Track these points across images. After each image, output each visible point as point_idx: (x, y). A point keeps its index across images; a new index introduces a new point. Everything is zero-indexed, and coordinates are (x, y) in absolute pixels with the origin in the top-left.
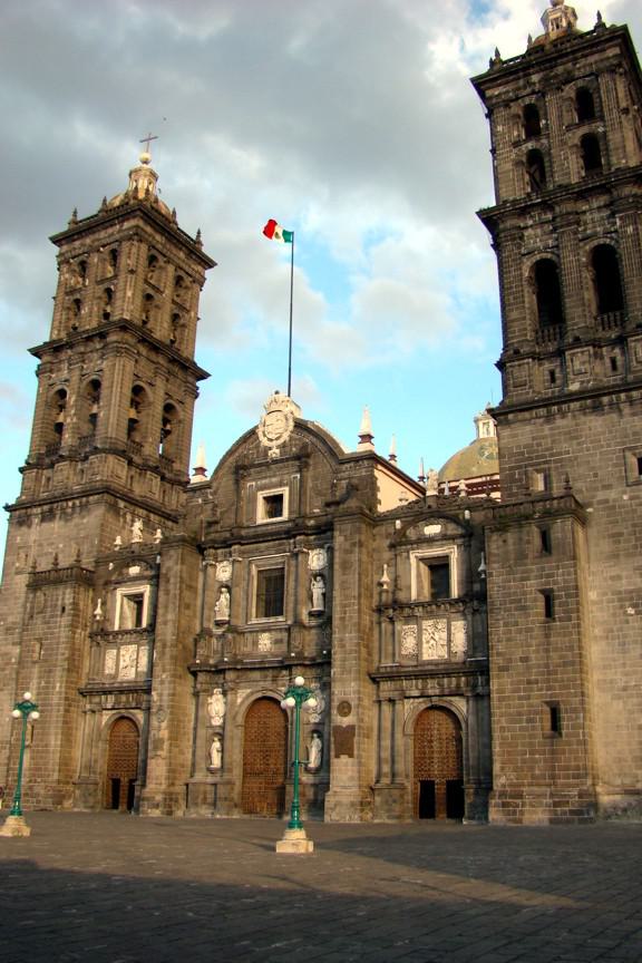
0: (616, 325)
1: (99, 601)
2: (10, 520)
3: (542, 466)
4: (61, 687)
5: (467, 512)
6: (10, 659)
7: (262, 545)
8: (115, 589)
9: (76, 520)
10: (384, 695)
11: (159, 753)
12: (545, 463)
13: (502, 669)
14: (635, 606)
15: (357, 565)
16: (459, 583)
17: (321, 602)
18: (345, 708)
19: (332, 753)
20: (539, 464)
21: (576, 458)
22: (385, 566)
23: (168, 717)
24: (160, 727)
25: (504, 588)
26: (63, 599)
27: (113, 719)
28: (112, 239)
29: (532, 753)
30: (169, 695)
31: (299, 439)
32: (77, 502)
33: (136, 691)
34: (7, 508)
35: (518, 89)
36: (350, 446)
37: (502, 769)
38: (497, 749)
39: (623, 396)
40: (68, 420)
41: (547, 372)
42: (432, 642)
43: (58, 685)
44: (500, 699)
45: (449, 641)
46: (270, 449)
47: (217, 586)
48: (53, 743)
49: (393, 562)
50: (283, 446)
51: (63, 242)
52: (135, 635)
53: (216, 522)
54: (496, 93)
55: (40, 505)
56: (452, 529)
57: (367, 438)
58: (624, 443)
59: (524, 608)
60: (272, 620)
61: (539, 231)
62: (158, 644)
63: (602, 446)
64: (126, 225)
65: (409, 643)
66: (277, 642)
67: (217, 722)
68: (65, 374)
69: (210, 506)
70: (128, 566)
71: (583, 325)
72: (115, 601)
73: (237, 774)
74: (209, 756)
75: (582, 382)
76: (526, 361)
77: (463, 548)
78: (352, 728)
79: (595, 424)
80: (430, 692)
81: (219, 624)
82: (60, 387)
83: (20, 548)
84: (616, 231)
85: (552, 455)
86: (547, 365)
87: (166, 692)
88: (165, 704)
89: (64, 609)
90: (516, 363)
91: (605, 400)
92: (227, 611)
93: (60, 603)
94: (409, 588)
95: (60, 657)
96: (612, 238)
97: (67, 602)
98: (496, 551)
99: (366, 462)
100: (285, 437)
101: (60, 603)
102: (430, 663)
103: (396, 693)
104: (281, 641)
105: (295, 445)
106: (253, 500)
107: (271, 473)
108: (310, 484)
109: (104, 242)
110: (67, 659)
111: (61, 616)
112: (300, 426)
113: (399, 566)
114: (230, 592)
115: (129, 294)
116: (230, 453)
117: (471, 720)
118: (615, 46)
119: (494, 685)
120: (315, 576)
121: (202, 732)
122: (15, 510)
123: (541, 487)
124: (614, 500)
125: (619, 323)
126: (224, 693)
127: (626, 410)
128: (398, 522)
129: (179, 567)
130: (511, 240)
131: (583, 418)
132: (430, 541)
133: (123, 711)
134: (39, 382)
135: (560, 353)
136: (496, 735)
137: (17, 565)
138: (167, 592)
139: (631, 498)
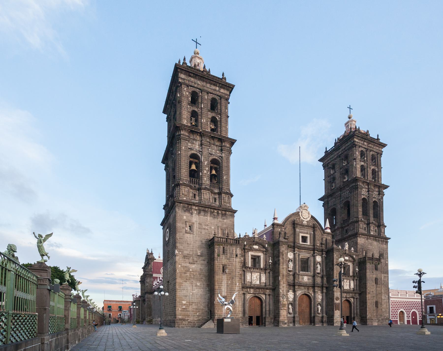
8: (248, 252)
13: (369, 293)
26: (236, 251)
40: (205, 172)
43: (238, 284)
48: (238, 304)
50: (307, 222)
59: (373, 281)
69: (283, 233)
89: (237, 256)
93: (234, 252)
95: (237, 273)
100: (309, 219)
101: (234, 252)
106: (299, 236)
110: (241, 275)
111: (236, 258)
112: (312, 217)
119: (367, 296)
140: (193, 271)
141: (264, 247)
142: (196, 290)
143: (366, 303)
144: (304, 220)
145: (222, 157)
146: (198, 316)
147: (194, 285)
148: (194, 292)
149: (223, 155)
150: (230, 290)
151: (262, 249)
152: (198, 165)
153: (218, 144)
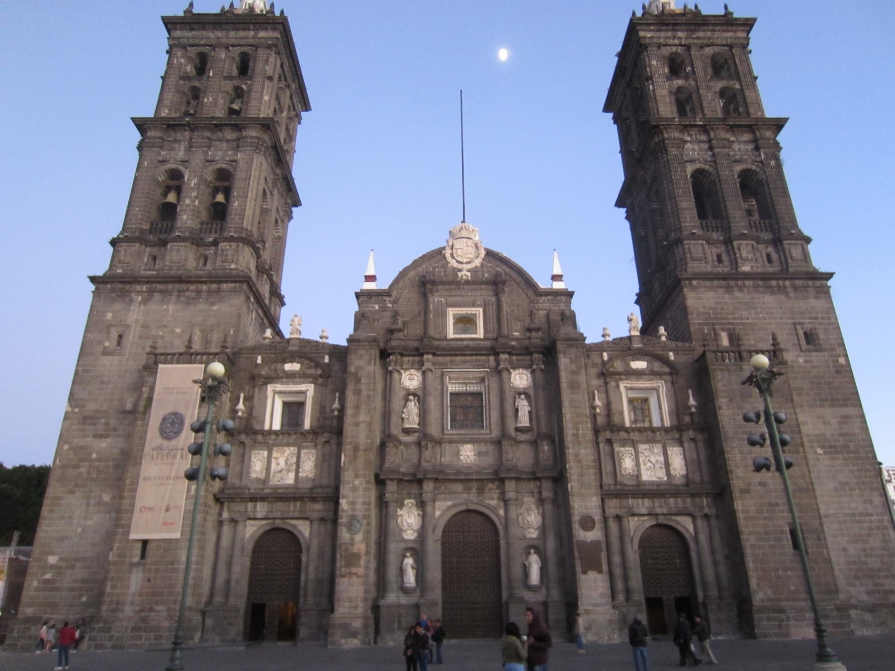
0: (766, 231)
1: (242, 395)
2: (96, 293)
3: (727, 326)
5: (671, 354)
6: (90, 454)
7: (459, 358)
8: (266, 384)
9: (201, 306)
10: (611, 511)
11: (354, 570)
12: (730, 323)
13: (746, 491)
14: (822, 447)
15: (585, 385)
16: (670, 414)
17: (527, 418)
18: (588, 523)
19: (578, 569)
20: (726, 324)
21: (756, 324)
22: (596, 392)
23: (364, 528)
24: (352, 540)
25: (734, 419)
27: (261, 531)
28: (244, 42)
29: (785, 569)
30: (365, 503)
31: (492, 267)
32: (205, 287)
33: (301, 499)
34: (93, 279)
35: (669, 38)
36: (543, 283)
37: (758, 584)
38: (750, 565)
39: (787, 283)
40: (188, 201)
41: (714, 255)
42: (649, 464)
44: (745, 519)
45: (667, 465)
46: (460, 270)
47: (402, 393)
49: (603, 389)
50: (473, 271)
51: (178, 26)
52: (293, 437)
53: (400, 330)
54: (649, 35)
55: (147, 282)
56: (657, 366)
57: (556, 278)
58: (794, 319)
60: (475, 431)
61: (696, 147)
62: (347, 447)
63: (776, 318)
64: (262, 34)
65: (628, 464)
66: (479, 454)
67: (410, 535)
68: (181, 154)
69: (387, 314)
70: (284, 361)
71: (743, 224)
72: (266, 398)
73: (436, 594)
74: (402, 571)
75: (752, 267)
76: (700, 242)
77: (669, 384)
78: (596, 544)
79: (769, 300)
80: (658, 511)
81: (407, 431)
82: (174, 166)
83: (109, 326)
84: (761, 162)
85: (735, 319)
86: (715, 250)
87: (360, 501)
88: (359, 513)
90: (692, 242)
91: (774, 283)
92: (416, 419)
94: (622, 413)
96: (757, 166)
98: (722, 388)
99: (564, 298)
100: (477, 262)
102: (652, 483)
103: (623, 510)
104: (486, 453)
105: (487, 272)
106: (444, 315)
107: (463, 293)
108: (505, 308)
109: (232, 41)
112: (490, 254)
113: (612, 395)
114: (419, 401)
115: (266, 98)
116: (416, 264)
118: (743, 31)
119: (738, 505)
120: (520, 394)
121: (394, 548)
122: (105, 283)
123: (725, 342)
124: (792, 361)
125: (768, 229)
126: (421, 504)
127: (792, 294)
128: (605, 354)
129: (372, 367)
130: (677, 147)
131: (756, 296)
132: (638, 374)
133: (278, 522)
134: (140, 156)
135: (728, 242)
136: (748, 551)
137: (107, 344)
138: (358, 392)
139: (806, 361)
140: (98, 460)
141: (318, 365)
142: (96, 517)
144: (460, 266)
145: (236, 161)
146: (87, 605)
147: (92, 502)
148: (90, 523)
149: (240, 156)
151: (312, 371)
152: (179, 190)
153: (230, 135)
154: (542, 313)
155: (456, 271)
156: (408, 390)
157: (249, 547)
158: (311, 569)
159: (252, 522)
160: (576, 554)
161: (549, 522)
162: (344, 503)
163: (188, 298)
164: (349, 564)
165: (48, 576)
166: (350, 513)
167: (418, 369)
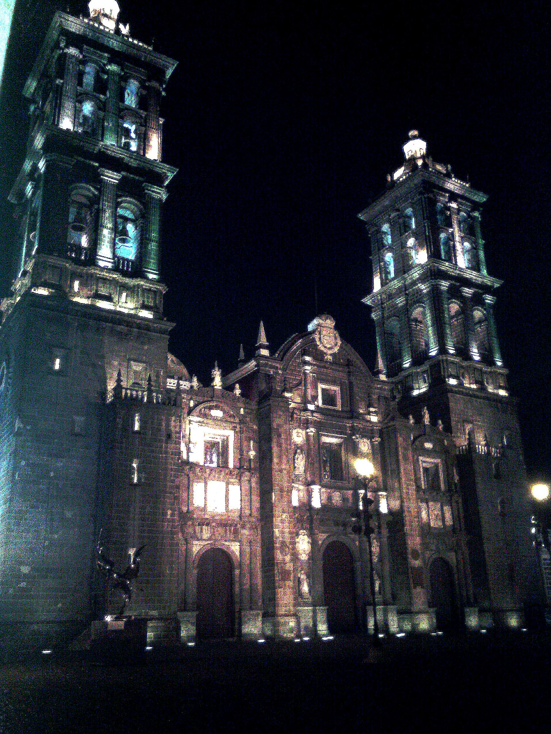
4: (172, 515)
6: (48, 472)
24: (284, 560)
26: (168, 425)
43: (169, 512)
50: (333, 355)
65: (424, 515)
70: (211, 408)
78: (420, 568)
87: (287, 530)
88: (288, 541)
95: (169, 484)
97: (173, 429)
100: (336, 350)
102: (436, 528)
117: (461, 566)
126: (311, 535)
143: (485, 565)
150: (150, 532)
154: (375, 397)
155: (322, 354)
156: (296, 445)
157: (196, 562)
158: (246, 580)
159: (197, 542)
160: (411, 575)
161: (386, 552)
162: (277, 532)
163: (120, 333)
164: (284, 579)
165: (23, 584)
166: (281, 539)
167: (302, 429)
